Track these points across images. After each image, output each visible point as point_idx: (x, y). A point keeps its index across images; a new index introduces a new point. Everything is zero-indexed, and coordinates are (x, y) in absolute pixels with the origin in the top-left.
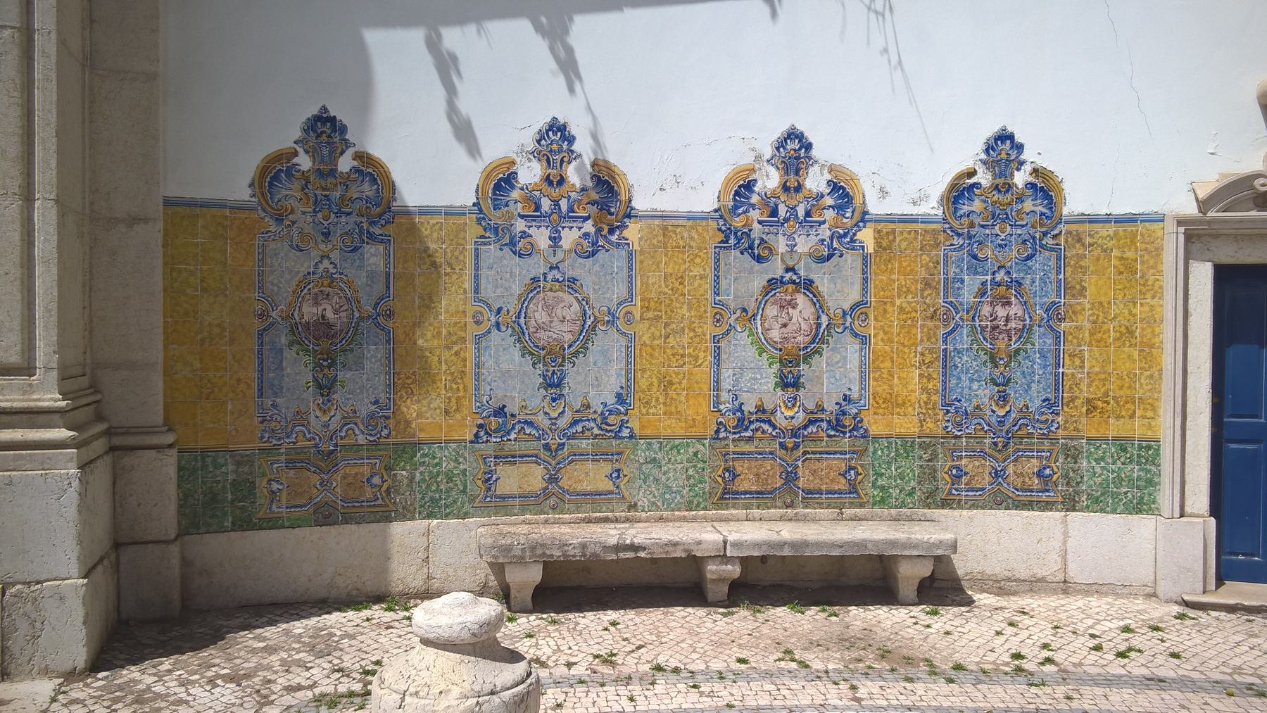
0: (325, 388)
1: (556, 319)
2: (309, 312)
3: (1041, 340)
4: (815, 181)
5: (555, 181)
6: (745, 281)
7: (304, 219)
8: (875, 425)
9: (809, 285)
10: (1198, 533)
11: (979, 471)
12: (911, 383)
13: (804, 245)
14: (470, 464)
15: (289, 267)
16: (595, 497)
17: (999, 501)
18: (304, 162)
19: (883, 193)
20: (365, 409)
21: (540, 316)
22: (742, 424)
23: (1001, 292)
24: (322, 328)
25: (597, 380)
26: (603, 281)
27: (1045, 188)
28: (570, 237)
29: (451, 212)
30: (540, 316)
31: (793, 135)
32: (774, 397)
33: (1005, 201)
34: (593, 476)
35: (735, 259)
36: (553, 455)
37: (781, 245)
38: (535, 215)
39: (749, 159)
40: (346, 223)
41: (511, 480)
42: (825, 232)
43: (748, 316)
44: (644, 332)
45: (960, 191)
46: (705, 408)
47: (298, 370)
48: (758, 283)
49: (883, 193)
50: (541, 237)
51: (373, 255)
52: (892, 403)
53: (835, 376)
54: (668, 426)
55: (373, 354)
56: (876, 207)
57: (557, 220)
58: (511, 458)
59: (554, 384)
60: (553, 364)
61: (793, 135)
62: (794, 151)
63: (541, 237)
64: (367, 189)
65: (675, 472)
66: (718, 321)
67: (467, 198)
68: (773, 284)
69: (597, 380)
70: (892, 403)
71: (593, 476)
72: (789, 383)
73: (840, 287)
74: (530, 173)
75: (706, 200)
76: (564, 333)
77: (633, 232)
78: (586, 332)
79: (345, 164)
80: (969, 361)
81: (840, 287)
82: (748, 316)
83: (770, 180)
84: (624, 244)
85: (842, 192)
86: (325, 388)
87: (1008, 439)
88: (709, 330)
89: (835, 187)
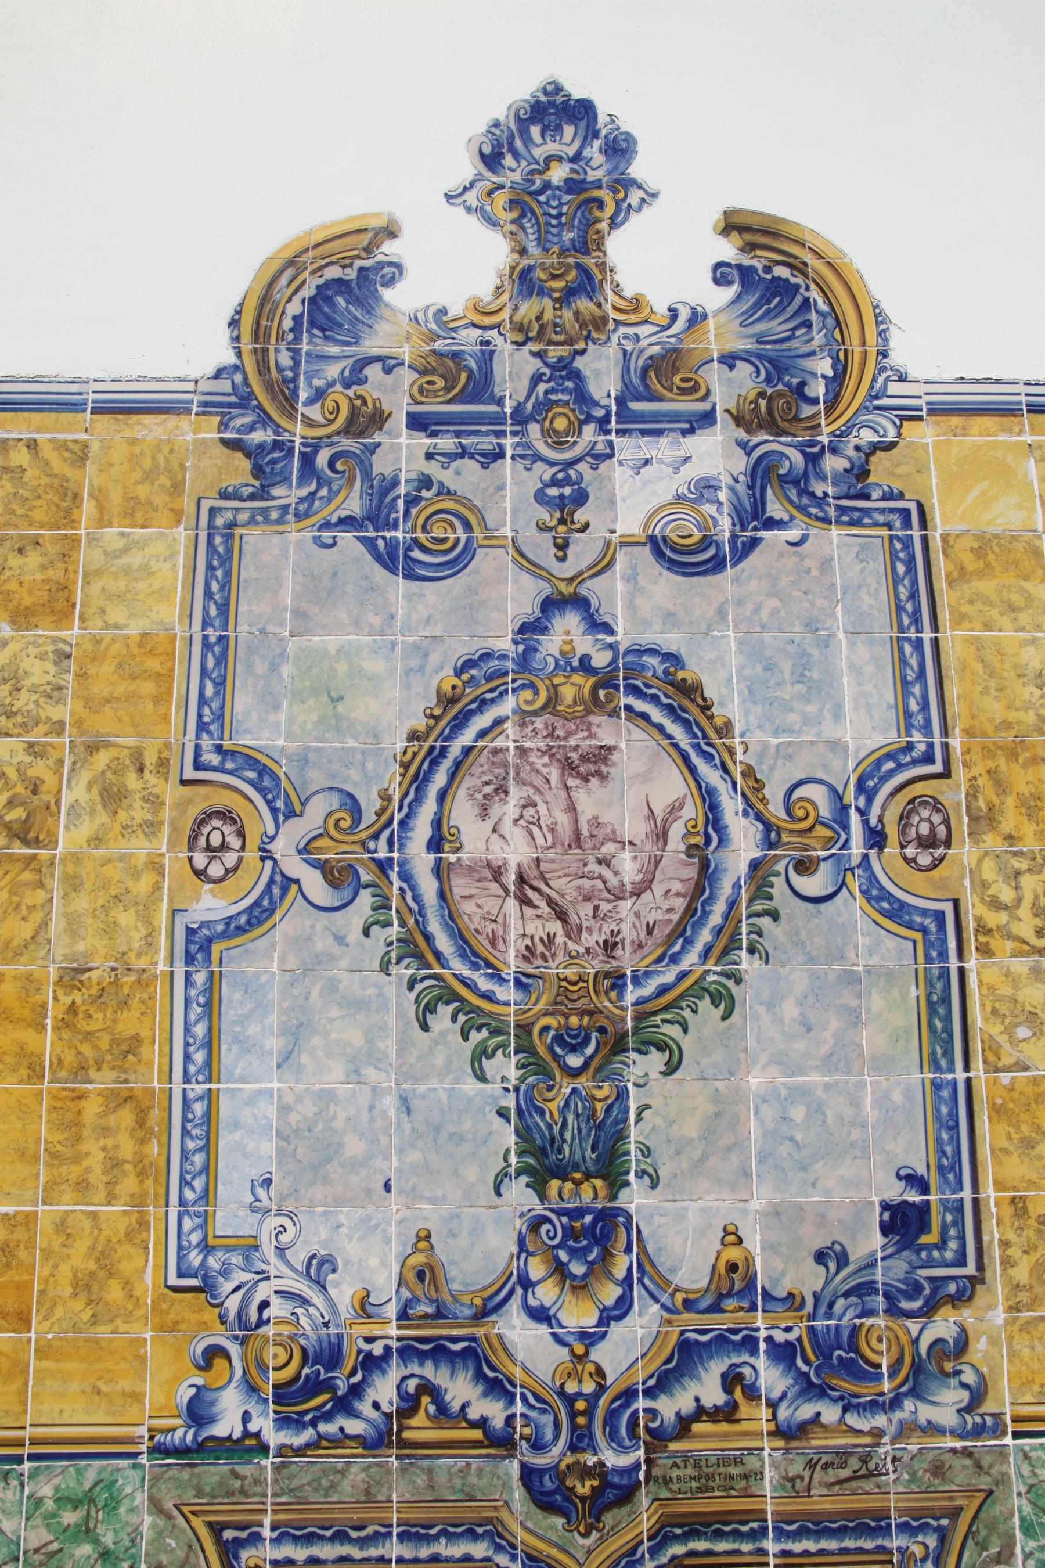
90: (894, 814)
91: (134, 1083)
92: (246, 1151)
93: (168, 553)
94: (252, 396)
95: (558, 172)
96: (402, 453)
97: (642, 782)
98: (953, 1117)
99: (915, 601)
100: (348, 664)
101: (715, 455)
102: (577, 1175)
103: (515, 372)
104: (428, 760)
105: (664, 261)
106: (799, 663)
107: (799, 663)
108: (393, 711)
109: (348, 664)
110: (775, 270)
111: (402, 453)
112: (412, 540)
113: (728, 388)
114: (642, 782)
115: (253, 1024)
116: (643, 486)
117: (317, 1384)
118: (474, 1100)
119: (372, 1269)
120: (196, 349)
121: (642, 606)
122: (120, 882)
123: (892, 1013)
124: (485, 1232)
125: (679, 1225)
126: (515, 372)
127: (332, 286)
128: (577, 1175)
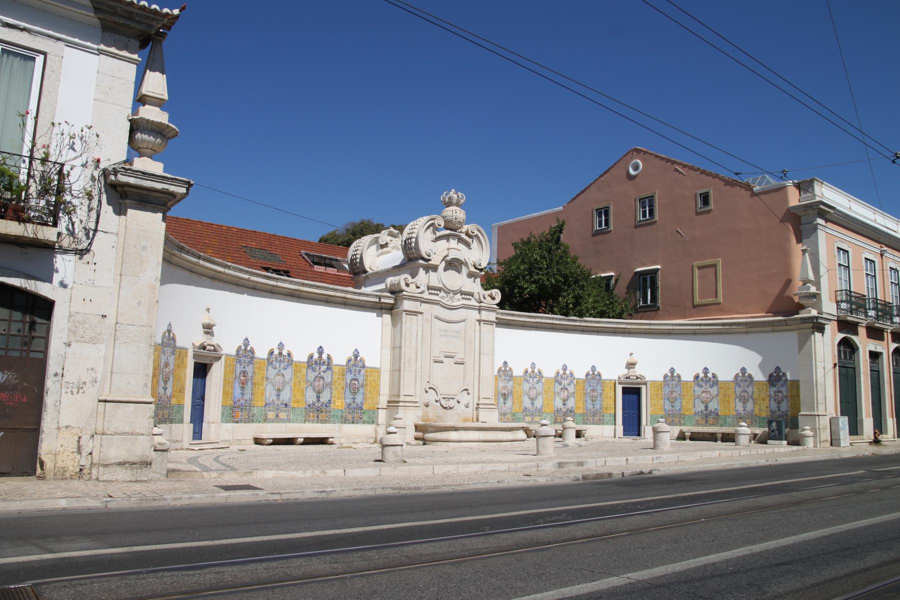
1: (533, 393)
3: (599, 398)
4: (568, 372)
6: (558, 388)
7: (503, 377)
8: (576, 411)
10: (620, 428)
11: (591, 418)
12: (581, 404)
13: (566, 382)
15: (501, 384)
17: (594, 424)
23: (593, 390)
24: (505, 394)
25: (538, 403)
26: (539, 387)
27: (599, 375)
32: (562, 407)
33: (594, 376)
35: (557, 384)
41: (528, 419)
45: (587, 375)
47: (502, 400)
52: (578, 408)
53: (571, 403)
54: (547, 411)
55: (510, 398)
60: (532, 400)
62: (565, 368)
67: (522, 374)
69: (538, 403)
70: (578, 408)
72: (564, 405)
73: (571, 389)
74: (530, 370)
76: (534, 396)
77: (543, 380)
80: (589, 401)
81: (571, 389)
83: (561, 372)
85: (571, 374)
87: (595, 414)
90: (330, 385)
94: (308, 362)
95: (321, 350)
97: (322, 382)
100: (312, 376)
102: (318, 397)
105: (324, 357)
106: (328, 377)
109: (312, 376)
110: (329, 357)
112: (314, 370)
114: (322, 382)
116: (324, 368)
117: (309, 406)
120: (306, 360)
121: (322, 374)
122: (303, 385)
124: (315, 400)
125: (322, 400)
127: (311, 357)
128: (318, 397)
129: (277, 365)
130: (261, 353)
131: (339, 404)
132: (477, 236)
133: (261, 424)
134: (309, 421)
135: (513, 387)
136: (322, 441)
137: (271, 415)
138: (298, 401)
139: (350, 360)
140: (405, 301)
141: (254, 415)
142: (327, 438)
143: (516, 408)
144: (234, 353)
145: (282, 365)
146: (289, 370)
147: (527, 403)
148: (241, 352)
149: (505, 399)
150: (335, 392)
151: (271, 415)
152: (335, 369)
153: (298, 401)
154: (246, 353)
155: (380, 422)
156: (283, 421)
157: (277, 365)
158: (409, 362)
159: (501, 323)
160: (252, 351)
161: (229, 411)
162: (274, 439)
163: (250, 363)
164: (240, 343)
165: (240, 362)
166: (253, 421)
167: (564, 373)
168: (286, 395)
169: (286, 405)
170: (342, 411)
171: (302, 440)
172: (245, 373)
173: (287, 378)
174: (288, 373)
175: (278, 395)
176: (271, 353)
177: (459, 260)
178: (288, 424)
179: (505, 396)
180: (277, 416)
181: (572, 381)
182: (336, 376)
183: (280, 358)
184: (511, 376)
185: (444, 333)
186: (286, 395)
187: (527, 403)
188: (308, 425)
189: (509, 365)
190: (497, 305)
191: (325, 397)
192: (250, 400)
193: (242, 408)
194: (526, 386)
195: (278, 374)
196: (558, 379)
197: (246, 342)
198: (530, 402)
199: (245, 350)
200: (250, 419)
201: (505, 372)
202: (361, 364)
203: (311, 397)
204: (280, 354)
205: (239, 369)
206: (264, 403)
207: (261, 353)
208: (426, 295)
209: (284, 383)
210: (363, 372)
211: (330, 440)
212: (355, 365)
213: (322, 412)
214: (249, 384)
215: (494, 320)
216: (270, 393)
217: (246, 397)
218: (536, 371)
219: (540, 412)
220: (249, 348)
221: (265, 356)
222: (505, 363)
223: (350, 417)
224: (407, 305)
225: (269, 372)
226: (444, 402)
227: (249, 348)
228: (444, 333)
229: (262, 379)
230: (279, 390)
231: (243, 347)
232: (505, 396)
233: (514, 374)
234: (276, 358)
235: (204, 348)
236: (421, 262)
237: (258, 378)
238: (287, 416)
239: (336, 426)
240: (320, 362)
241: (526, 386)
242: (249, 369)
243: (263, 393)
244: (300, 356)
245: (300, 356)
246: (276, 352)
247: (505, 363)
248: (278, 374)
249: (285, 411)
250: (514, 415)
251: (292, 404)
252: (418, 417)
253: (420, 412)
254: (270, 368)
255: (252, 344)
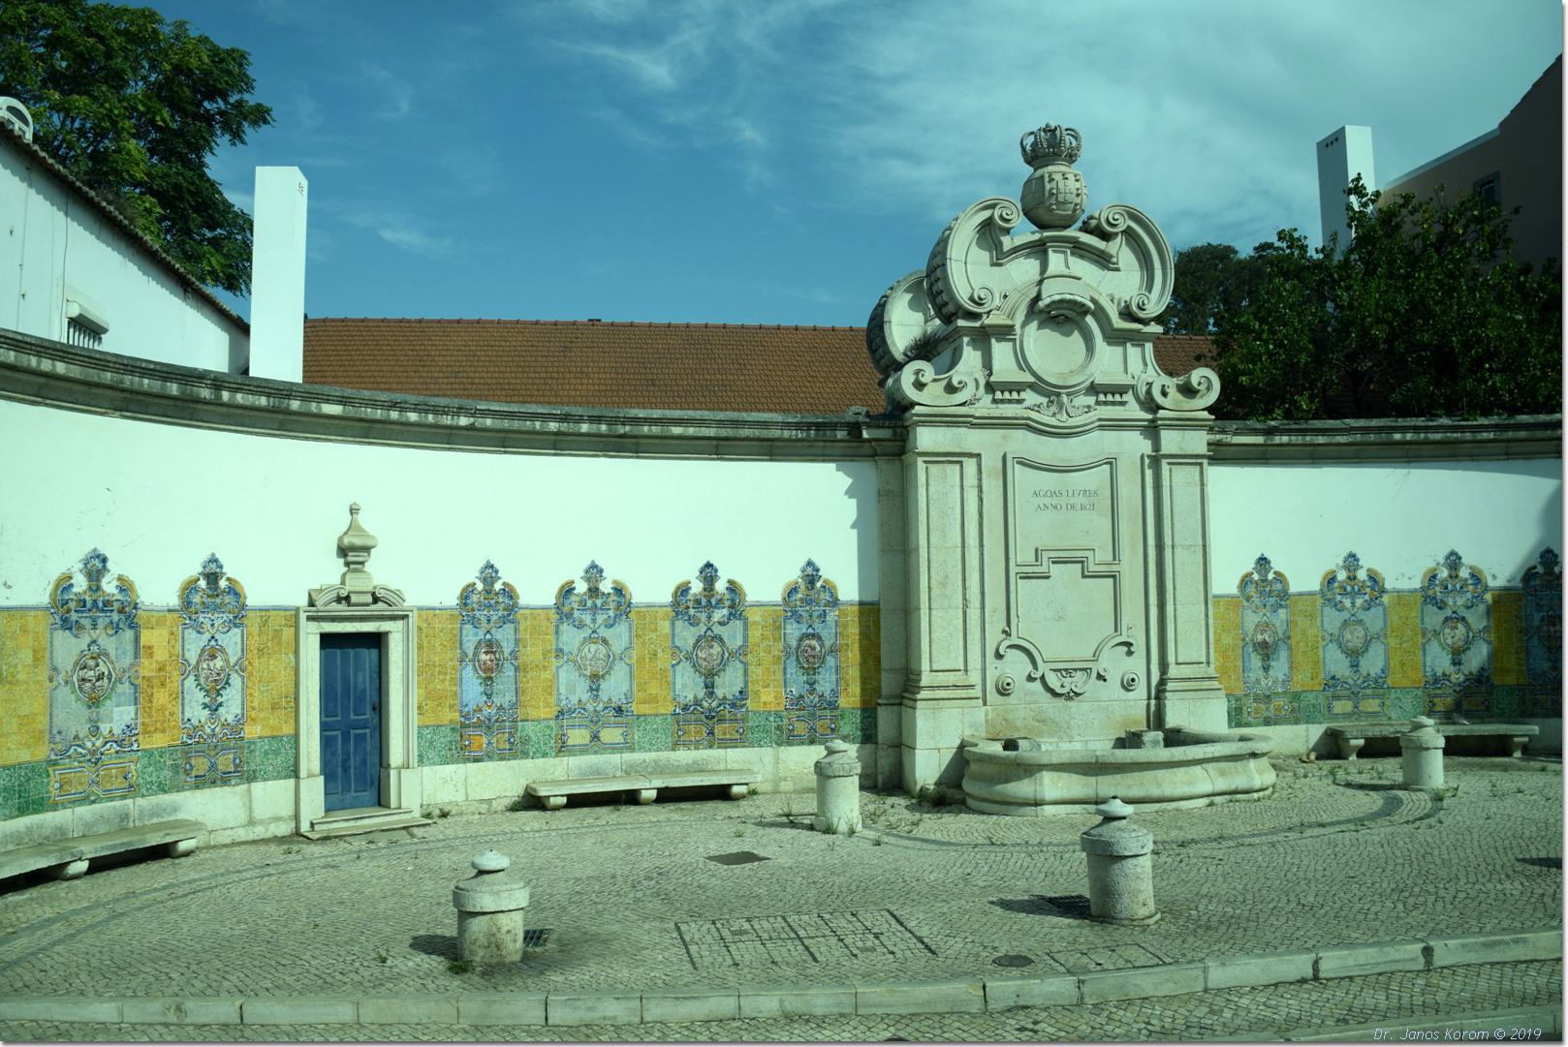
0: (1266, 669)
1: (1354, 637)
2: (1260, 638)
4: (1464, 573)
5: (1352, 578)
6: (1434, 618)
7: (1256, 600)
9: (1463, 619)
13: (1460, 601)
14: (1322, 700)
15: (1252, 620)
16: (1375, 714)
18: (1256, 577)
19: (1494, 577)
20: (1281, 677)
21: (1348, 636)
22: (1436, 681)
24: (1264, 645)
25: (1373, 663)
26: (1374, 620)
28: (1359, 602)
29: (1311, 594)
30: (1348, 636)
31: (1453, 553)
32: (1449, 668)
34: (1373, 705)
35: (1431, 609)
36: (1354, 695)
37: (1450, 602)
38: (1344, 593)
39: (1433, 565)
40: (1272, 600)
41: (1342, 706)
42: (1469, 595)
43: (1436, 634)
44: (1393, 642)
46: (1420, 674)
47: (1256, 661)
48: (1441, 619)
49: (1494, 577)
50: (1347, 602)
51: (1282, 612)
55: (1283, 654)
56: (1491, 583)
57: (1353, 595)
58: (1337, 698)
59: (1355, 666)
60: (1354, 655)
61: (1453, 553)
62: (1454, 561)
63: (1347, 602)
64: (1279, 586)
65: (1408, 702)
66: (1424, 635)
67: (1316, 587)
68: (1447, 619)
69: (1373, 663)
71: (1373, 705)
72: (1456, 663)
74: (1342, 576)
75: (1416, 584)
77: (1385, 599)
78: (1367, 644)
79: (1271, 576)
82: (1436, 634)
83: (1444, 573)
84: (1381, 604)
86: (1266, 669)
88: (1420, 640)
89: (1473, 575)
90: (743, 651)
91: (666, 679)
92: (678, 686)
93: (667, 624)
95: (709, 573)
96: (692, 611)
97: (717, 649)
98: (746, 683)
99: (746, 629)
100: (687, 636)
101: (725, 612)
102: (710, 687)
103: (704, 601)
104: (695, 646)
105: (720, 586)
106: (733, 634)
107: (733, 634)
108: (691, 641)
109: (687, 636)
110: (733, 588)
111: (692, 611)
112: (693, 622)
113: (727, 603)
114: (717, 649)
115: (678, 675)
116: (719, 614)
117: (685, 708)
118: (700, 681)
119: (691, 697)
120: (668, 599)
121: (717, 630)
122: (664, 660)
123: (741, 672)
124: (701, 694)
125: (719, 692)
126: (704, 601)
127: (683, 590)
128: (710, 687)
129: (587, 618)
130: (536, 592)
131: (768, 697)
132: (1129, 233)
133: (551, 761)
134: (687, 745)
135: (1288, 622)
136: (721, 793)
137: (578, 736)
138: (654, 700)
139: (792, 591)
140: (919, 430)
141: (526, 741)
142: (729, 786)
143: (1302, 680)
144: (452, 600)
145: (601, 618)
146: (622, 628)
147: (1337, 663)
148: (475, 598)
149: (1266, 658)
150: (756, 672)
151: (578, 736)
152: (754, 616)
153: (654, 700)
154: (489, 599)
155: (881, 738)
156: (614, 748)
157: (587, 618)
158: (943, 584)
159: (1220, 455)
160: (509, 592)
161: (445, 737)
162: (569, 797)
163: (504, 620)
164: (471, 575)
165: (475, 622)
166: (525, 755)
167: (1454, 577)
168: (615, 687)
169: (619, 710)
170: (778, 715)
171: (653, 794)
172: (491, 646)
173: (617, 647)
174: (619, 636)
175: (595, 690)
176: (567, 591)
177: (1074, 303)
178: (628, 756)
179: (1266, 650)
180: (595, 737)
181: (1479, 597)
182: (755, 634)
183: (595, 600)
184: (1284, 595)
185: (1048, 501)
186: (615, 687)
187: (1337, 663)
188: (684, 756)
189: (1277, 565)
190: (1210, 409)
191: (729, 684)
192: (514, 706)
193: (487, 726)
194: (1332, 620)
195: (590, 640)
196: (1432, 592)
197: (489, 573)
198: (1347, 663)
199: (488, 591)
200: (516, 749)
201: (1264, 583)
202: (825, 596)
203: (688, 685)
204: (594, 591)
205: (471, 638)
206: (554, 711)
207: (536, 592)
208: (985, 407)
209: (610, 660)
210: (832, 615)
211: (735, 790)
212: (808, 601)
213: (721, 721)
214: (509, 671)
215: (1203, 449)
216: (572, 687)
217: (497, 700)
218: (1362, 575)
219: (1378, 686)
220: (498, 586)
221: (549, 599)
222: (1263, 562)
223: (801, 728)
224: (926, 438)
225: (564, 638)
226: (1053, 681)
227: (498, 586)
228: (1048, 501)
229: (546, 653)
230: (595, 677)
231: (480, 586)
232: (1266, 650)
233: (1293, 589)
234: (583, 603)
235: (347, 598)
236: (961, 323)
237: (532, 653)
238: (625, 735)
239: (767, 753)
240: (708, 600)
241: (1332, 620)
242: (505, 636)
243: (551, 687)
244: (652, 589)
245: (652, 589)
246: (581, 587)
247: (1263, 562)
248: (590, 640)
249: (617, 725)
250: (1296, 697)
251: (634, 708)
252: (972, 725)
253: (979, 714)
254: (564, 627)
255: (507, 575)
